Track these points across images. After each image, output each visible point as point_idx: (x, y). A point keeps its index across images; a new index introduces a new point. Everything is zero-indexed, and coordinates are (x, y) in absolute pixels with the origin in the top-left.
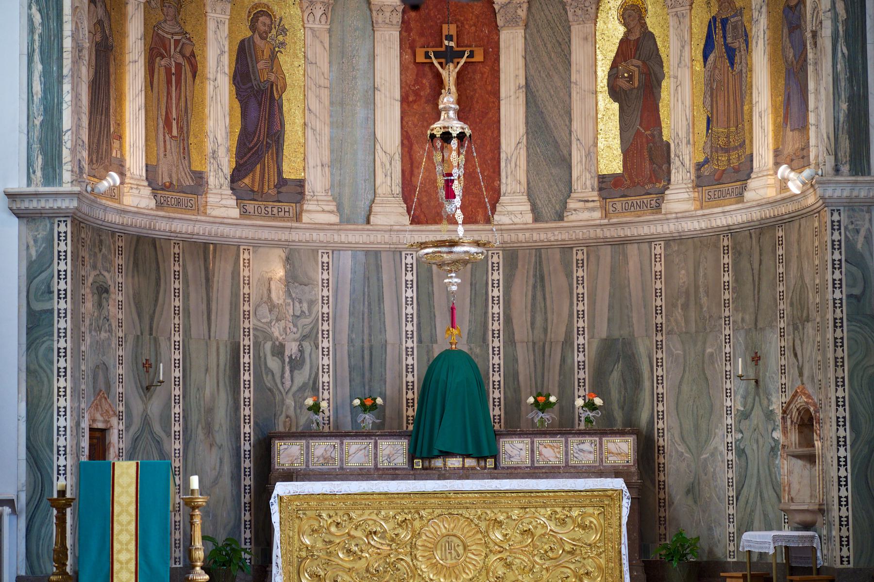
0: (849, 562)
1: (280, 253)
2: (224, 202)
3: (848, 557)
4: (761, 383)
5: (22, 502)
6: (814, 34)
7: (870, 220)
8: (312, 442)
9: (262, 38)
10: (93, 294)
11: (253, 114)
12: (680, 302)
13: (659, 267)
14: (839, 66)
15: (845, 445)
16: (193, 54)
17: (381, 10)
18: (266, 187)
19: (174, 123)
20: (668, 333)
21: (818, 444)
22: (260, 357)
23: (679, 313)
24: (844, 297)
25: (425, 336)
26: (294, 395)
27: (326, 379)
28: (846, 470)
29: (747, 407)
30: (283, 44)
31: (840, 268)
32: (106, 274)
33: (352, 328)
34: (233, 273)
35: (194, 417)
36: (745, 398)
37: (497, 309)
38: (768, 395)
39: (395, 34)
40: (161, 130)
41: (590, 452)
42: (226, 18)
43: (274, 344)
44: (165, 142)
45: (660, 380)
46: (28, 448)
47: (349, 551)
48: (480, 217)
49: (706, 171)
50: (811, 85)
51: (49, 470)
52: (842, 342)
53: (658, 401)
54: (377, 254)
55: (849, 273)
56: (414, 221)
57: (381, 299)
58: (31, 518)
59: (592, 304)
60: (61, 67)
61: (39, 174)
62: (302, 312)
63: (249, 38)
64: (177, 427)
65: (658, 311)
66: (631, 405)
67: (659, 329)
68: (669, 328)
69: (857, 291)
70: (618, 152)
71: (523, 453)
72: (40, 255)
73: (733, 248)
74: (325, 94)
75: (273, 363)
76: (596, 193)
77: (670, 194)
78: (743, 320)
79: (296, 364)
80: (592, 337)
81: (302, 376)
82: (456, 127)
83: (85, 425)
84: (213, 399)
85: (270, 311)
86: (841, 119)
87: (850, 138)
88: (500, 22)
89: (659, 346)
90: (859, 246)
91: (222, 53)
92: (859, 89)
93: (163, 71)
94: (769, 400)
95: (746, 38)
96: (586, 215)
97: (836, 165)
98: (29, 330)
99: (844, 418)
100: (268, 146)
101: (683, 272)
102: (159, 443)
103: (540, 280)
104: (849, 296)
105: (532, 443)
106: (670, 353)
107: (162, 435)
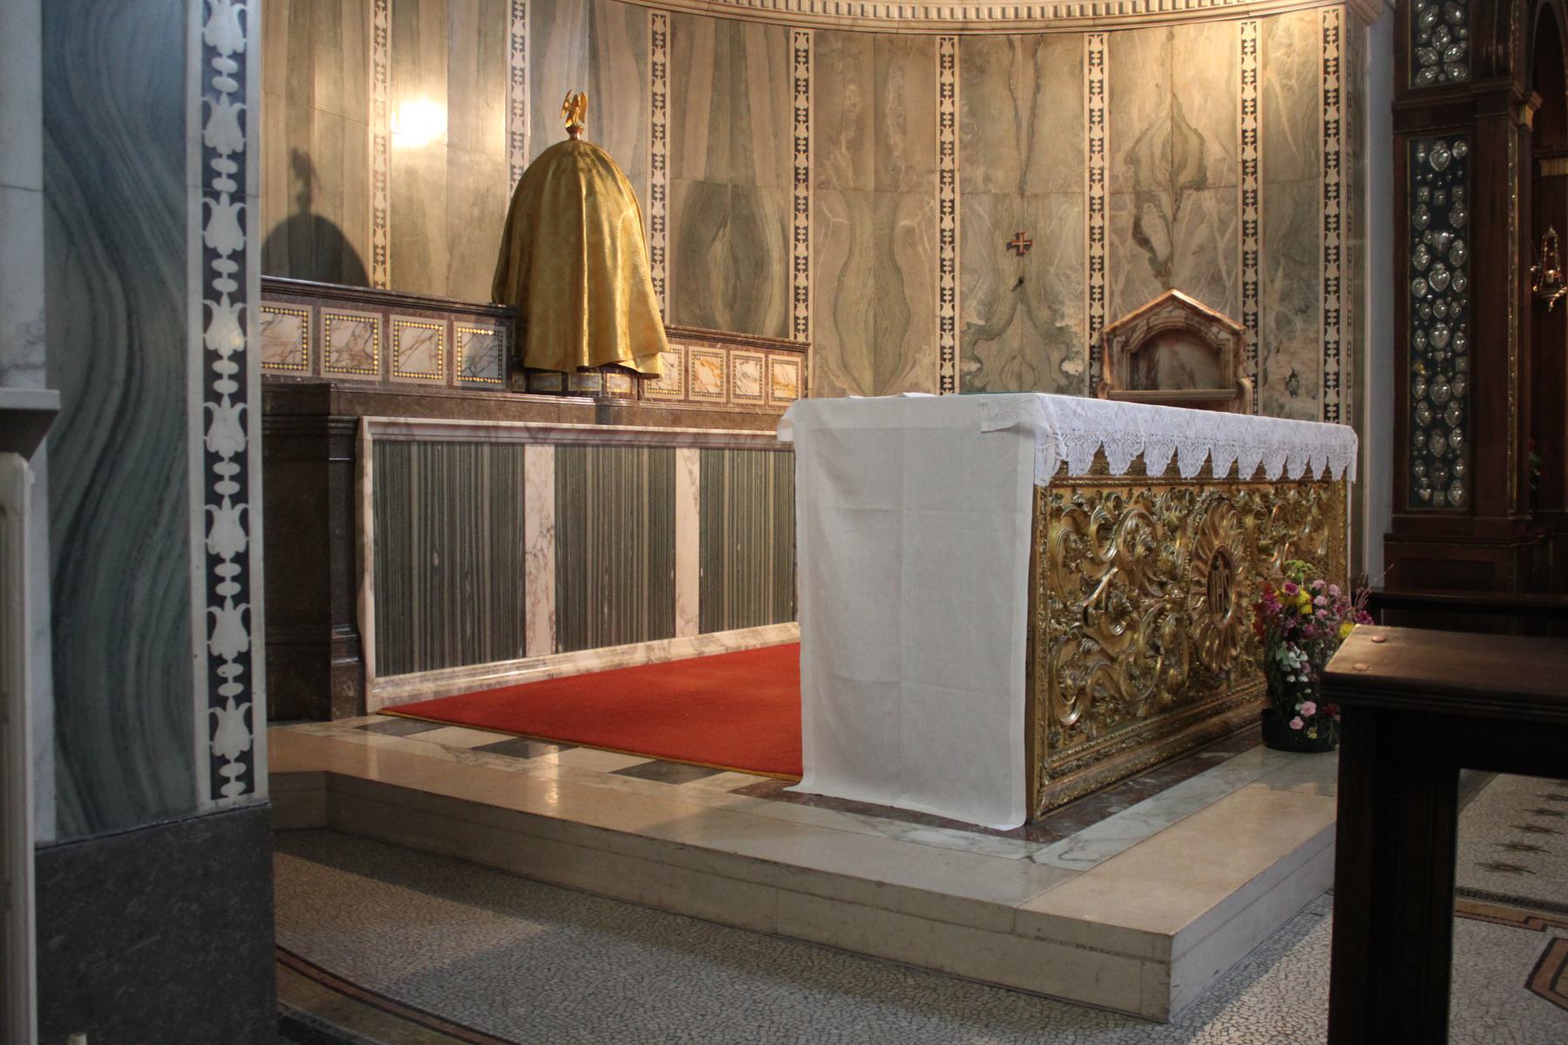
4: (1031, 286)
12: (851, 133)
20: (820, 186)
23: (842, 156)
29: (995, 320)
36: (989, 307)
38: (1053, 304)
41: (755, 380)
45: (801, 265)
46: (52, 127)
51: (166, 270)
53: (797, 300)
58: (76, 521)
67: (800, 177)
68: (822, 178)
71: (675, 373)
73: (963, 61)
78: (987, 179)
80: (676, 176)
89: (800, 207)
94: (1055, 312)
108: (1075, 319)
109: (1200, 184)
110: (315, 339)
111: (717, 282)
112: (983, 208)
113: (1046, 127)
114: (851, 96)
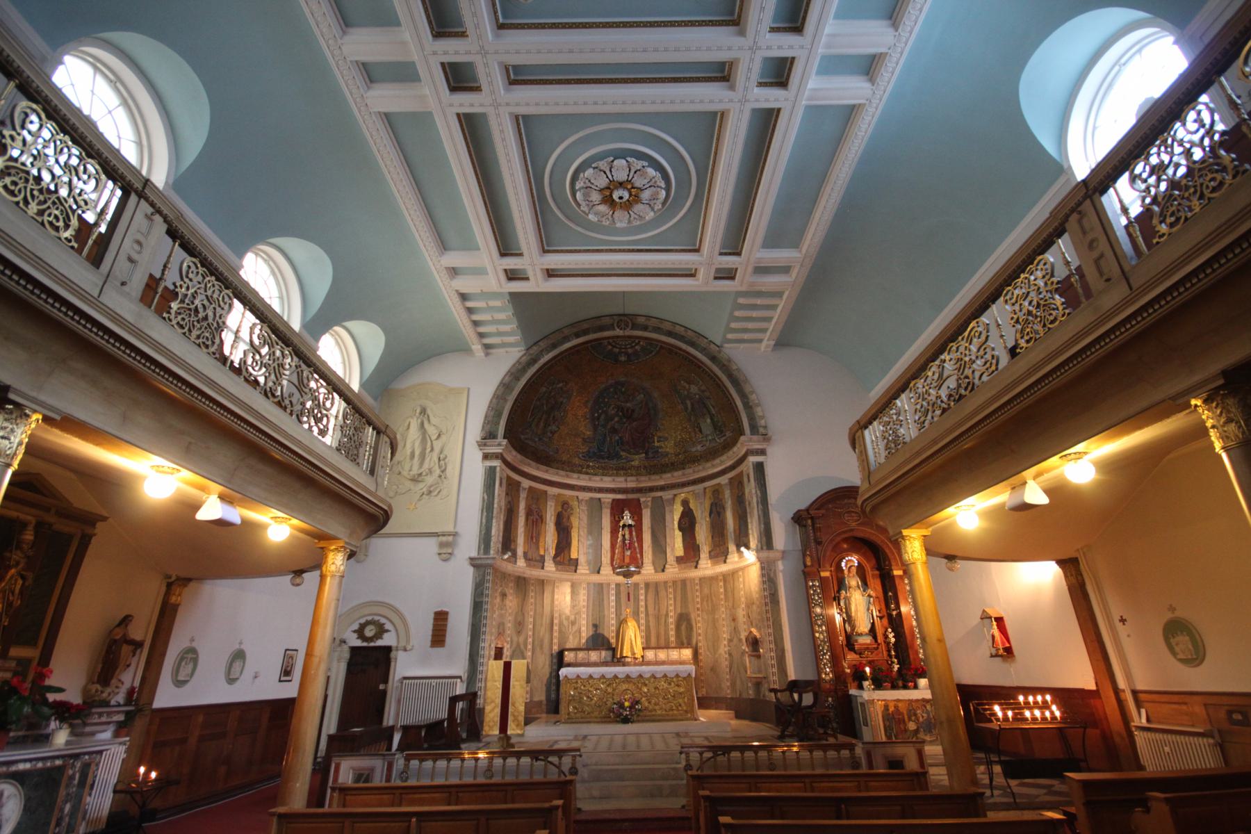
1: (569, 584)
5: (465, 677)
6: (749, 504)
8: (578, 652)
13: (698, 587)
20: (702, 611)
21: (761, 650)
23: (705, 603)
25: (618, 613)
33: (593, 610)
35: (536, 643)
37: (642, 603)
38: (739, 633)
39: (609, 511)
42: (553, 504)
45: (699, 628)
47: (588, 697)
49: (712, 554)
50: (749, 520)
55: (769, 586)
60: (492, 513)
61: (482, 551)
64: (530, 647)
65: (698, 603)
66: (689, 638)
67: (698, 609)
69: (772, 592)
70: (682, 548)
72: (480, 581)
74: (586, 530)
77: (700, 562)
79: (573, 623)
81: (575, 628)
82: (630, 522)
83: (493, 646)
89: (698, 615)
90: (772, 575)
95: (724, 508)
96: (671, 570)
98: (474, 609)
103: (657, 593)
108: (743, 635)
109: (753, 603)
112: (728, 611)
114: (706, 591)
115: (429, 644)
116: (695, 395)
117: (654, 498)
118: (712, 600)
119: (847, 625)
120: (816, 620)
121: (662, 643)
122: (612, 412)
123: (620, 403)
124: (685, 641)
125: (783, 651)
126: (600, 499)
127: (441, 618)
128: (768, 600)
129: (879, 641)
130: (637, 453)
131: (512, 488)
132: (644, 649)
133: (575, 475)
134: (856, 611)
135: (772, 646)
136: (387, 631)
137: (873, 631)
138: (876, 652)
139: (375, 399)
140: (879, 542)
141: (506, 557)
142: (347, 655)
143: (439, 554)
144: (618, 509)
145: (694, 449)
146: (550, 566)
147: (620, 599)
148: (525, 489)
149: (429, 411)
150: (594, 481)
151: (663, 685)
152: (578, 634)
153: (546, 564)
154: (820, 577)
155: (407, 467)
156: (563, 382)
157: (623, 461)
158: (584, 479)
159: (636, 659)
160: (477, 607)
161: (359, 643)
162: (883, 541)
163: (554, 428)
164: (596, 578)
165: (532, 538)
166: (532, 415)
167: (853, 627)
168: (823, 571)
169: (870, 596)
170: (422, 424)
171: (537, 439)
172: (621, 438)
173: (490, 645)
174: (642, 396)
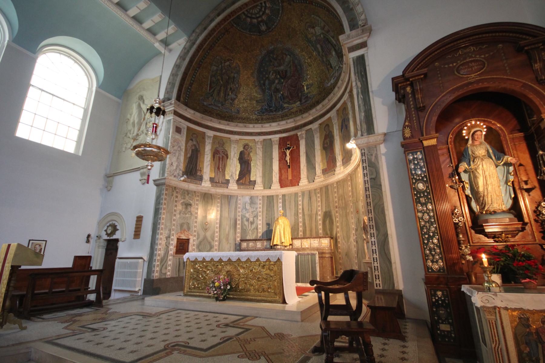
0: (380, 286)
2: (233, 186)
3: (379, 284)
7: (377, 150)
9: (246, 150)
10: (182, 205)
11: (243, 166)
13: (336, 190)
14: (360, 102)
15: (374, 236)
16: (227, 154)
17: (274, 141)
18: (246, 183)
19: (221, 169)
22: (242, 222)
23: (340, 201)
24: (369, 179)
26: (252, 231)
27: (260, 226)
28: (375, 246)
30: (251, 151)
31: (366, 169)
32: (190, 201)
33: (267, 214)
34: (236, 202)
37: (300, 207)
39: (277, 146)
40: (216, 170)
43: (246, 219)
44: (217, 173)
47: (202, 277)
48: (297, 184)
52: (369, 196)
54: (273, 196)
55: (370, 171)
56: (281, 187)
57: (274, 207)
59: (322, 203)
61: (161, 175)
62: (254, 211)
63: (243, 151)
66: (331, 230)
69: (373, 177)
74: (261, 161)
75: (246, 223)
76: (322, 174)
79: (252, 223)
80: (322, 212)
81: (254, 226)
84: (229, 232)
85: (246, 211)
86: (362, 119)
87: (366, 124)
88: (300, 139)
90: (373, 160)
91: (235, 153)
92: (368, 107)
93: (218, 158)
96: (319, 180)
97: (362, 134)
99: (373, 225)
100: (247, 173)
101: (341, 190)
102: (210, 243)
103: (310, 198)
104: (371, 179)
105: (301, 241)
106: (339, 213)
107: (211, 241)
110: (248, 245)
111: (328, 227)
113: (357, 188)
114: (341, 191)
115: (133, 236)
116: (320, 35)
117: (307, 131)
118: (345, 198)
119: (473, 204)
120: (418, 198)
121: (314, 234)
122: (272, 77)
123: (275, 68)
124: (329, 232)
125: (386, 236)
126: (270, 139)
127: (139, 219)
128: (369, 185)
129: (526, 220)
130: (295, 103)
131: (192, 135)
132: (292, 239)
133: (251, 125)
134: (486, 184)
135: (373, 231)
136: (118, 230)
137: (515, 209)
138: (520, 233)
139: (120, 97)
140: (517, 88)
141: (182, 179)
142: (105, 244)
143: (140, 180)
144: (284, 144)
145: (329, 84)
146: (233, 187)
147: (285, 205)
148: (210, 137)
149: (144, 98)
150: (265, 127)
151: (257, 269)
152: (255, 230)
153: (229, 185)
154: (424, 148)
155: (132, 132)
156: (228, 60)
157: (286, 111)
158: (258, 127)
159: (286, 246)
160: (157, 211)
161: (106, 237)
162: (525, 85)
163: (233, 96)
164: (268, 192)
165: (219, 168)
166: (211, 88)
167: (482, 205)
168: (426, 140)
169: (507, 164)
170: (139, 106)
171: (220, 105)
172: (282, 95)
173: (168, 238)
174: (289, 57)
